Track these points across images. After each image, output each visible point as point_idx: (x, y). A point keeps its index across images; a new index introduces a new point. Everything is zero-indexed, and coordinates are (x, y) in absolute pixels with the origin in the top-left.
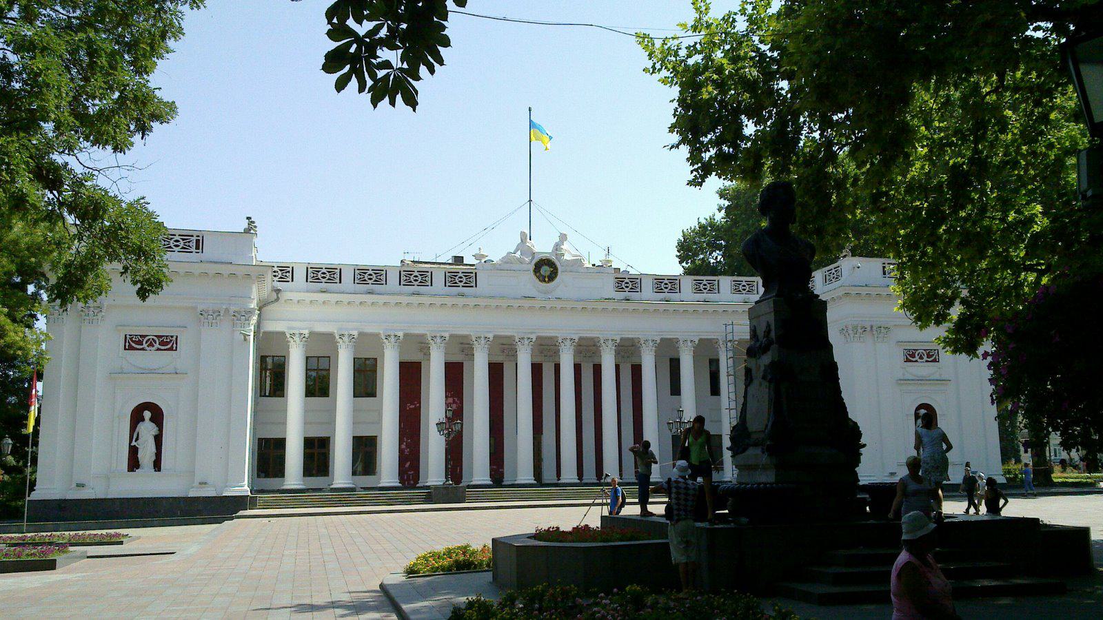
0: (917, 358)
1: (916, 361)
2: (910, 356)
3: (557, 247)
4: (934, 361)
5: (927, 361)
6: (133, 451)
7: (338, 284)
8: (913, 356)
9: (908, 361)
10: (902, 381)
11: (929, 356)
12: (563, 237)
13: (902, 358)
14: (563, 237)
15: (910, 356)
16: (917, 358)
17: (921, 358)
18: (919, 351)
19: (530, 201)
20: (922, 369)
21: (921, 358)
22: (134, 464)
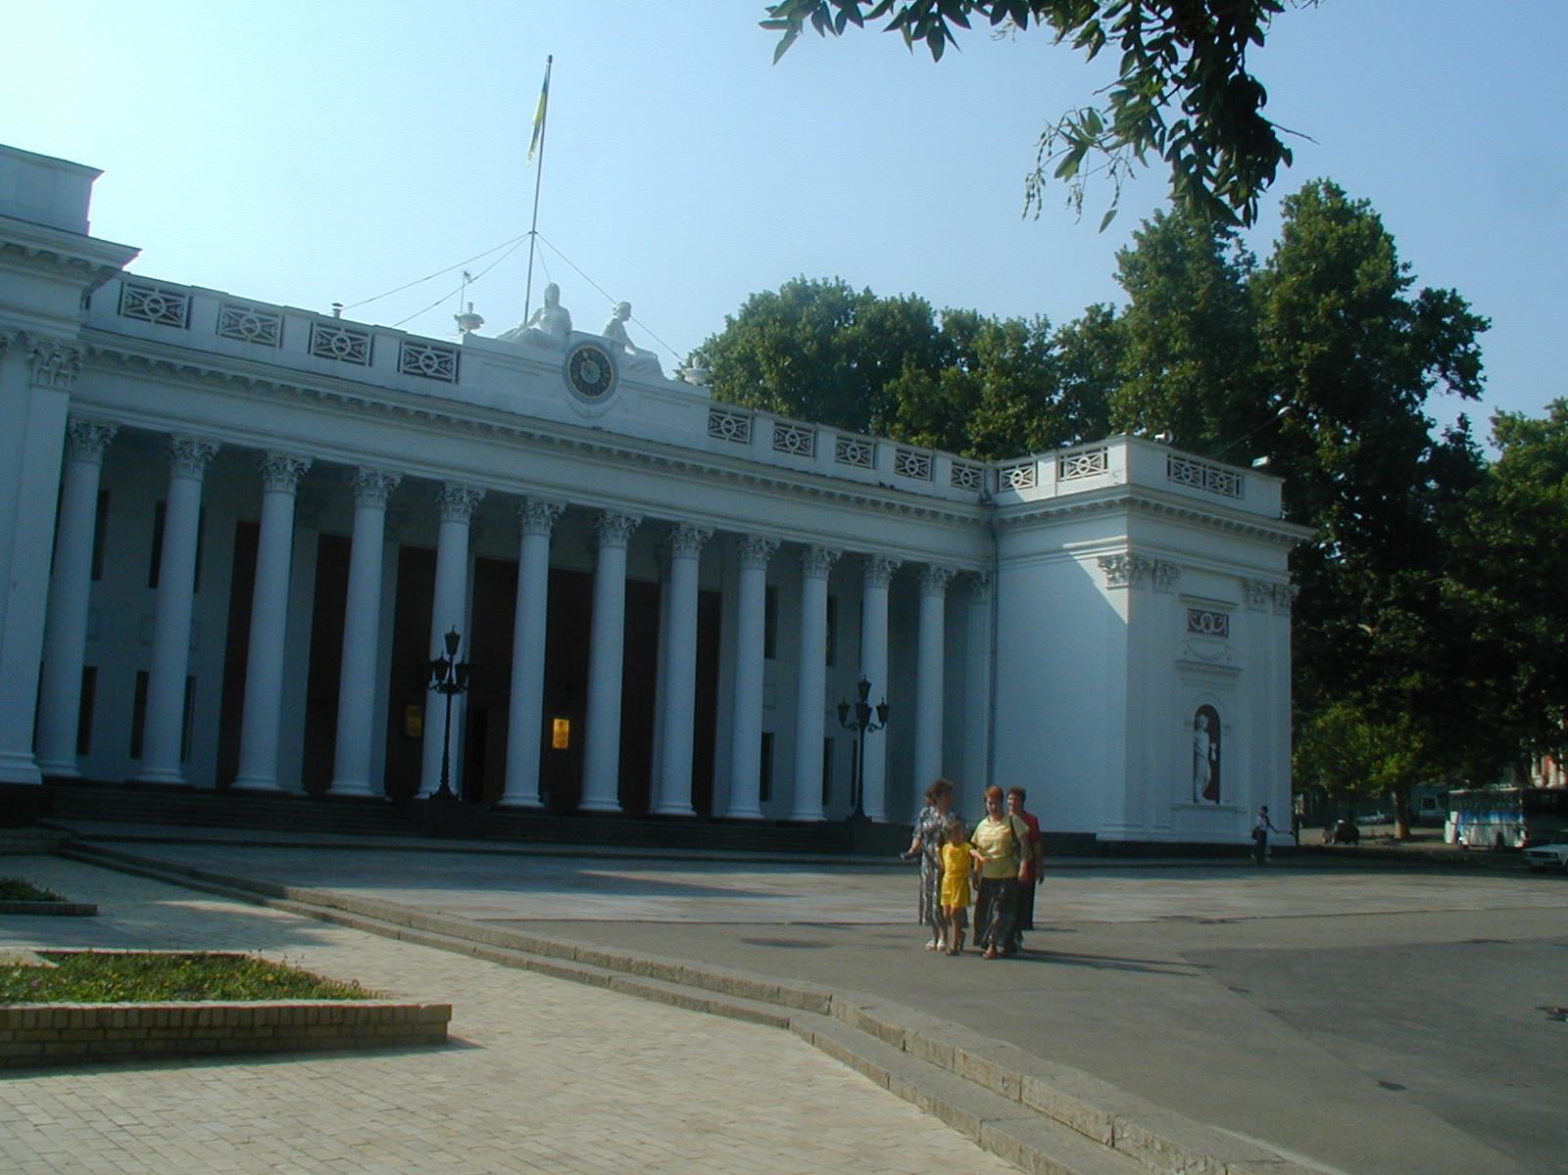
1: (1201, 631)
3: (616, 327)
4: (1224, 634)
5: (1214, 633)
7: (183, 330)
10: (1183, 665)
11: (1217, 625)
12: (625, 311)
13: (1186, 626)
14: (625, 311)
17: (1207, 627)
19: (534, 232)
20: (1206, 646)
21: (1207, 627)
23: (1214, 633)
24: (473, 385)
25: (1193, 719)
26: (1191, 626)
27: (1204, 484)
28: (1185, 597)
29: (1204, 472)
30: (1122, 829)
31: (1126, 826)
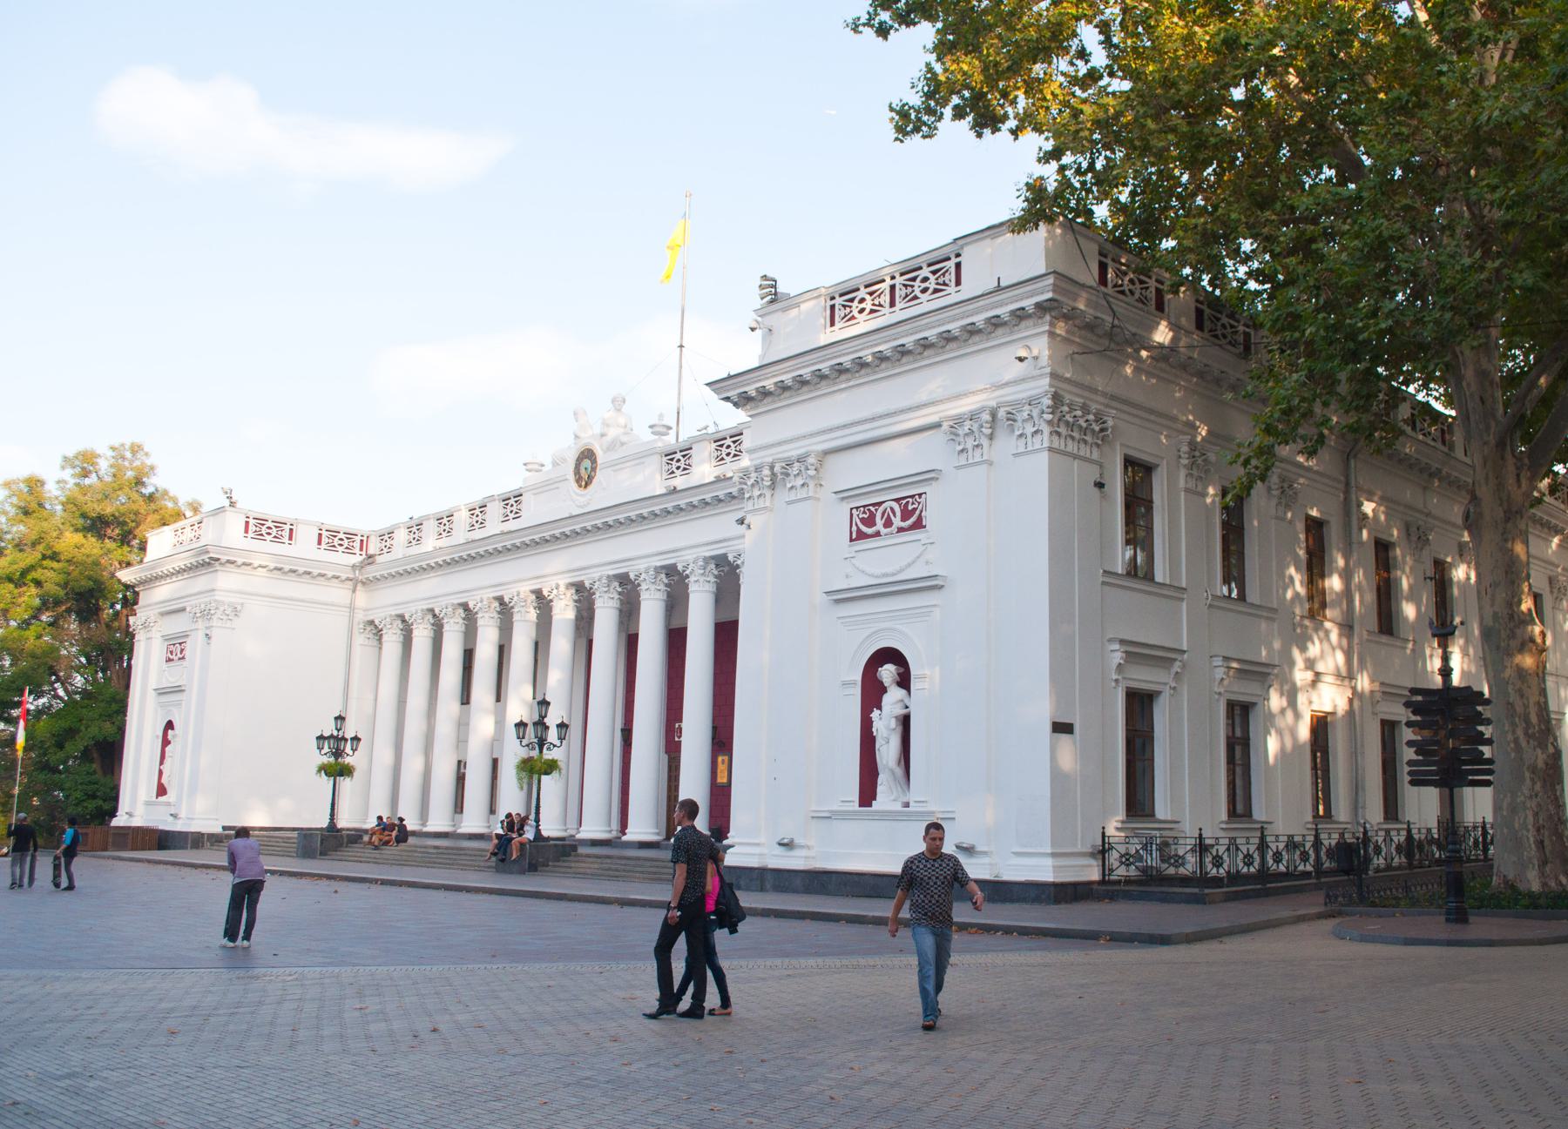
0: (880, 522)
1: (878, 534)
2: (865, 526)
4: (919, 525)
5: (901, 530)
6: (161, 773)
8: (870, 522)
9: (861, 536)
10: (842, 598)
11: (906, 515)
15: (865, 526)
16: (880, 522)
17: (888, 524)
18: (881, 509)
20: (890, 556)
21: (888, 524)
22: (162, 791)
23: (901, 530)
24: (535, 512)
25: (858, 677)
26: (859, 530)
27: (892, 304)
28: (844, 495)
29: (893, 287)
30: (1049, 862)
31: (1054, 855)
